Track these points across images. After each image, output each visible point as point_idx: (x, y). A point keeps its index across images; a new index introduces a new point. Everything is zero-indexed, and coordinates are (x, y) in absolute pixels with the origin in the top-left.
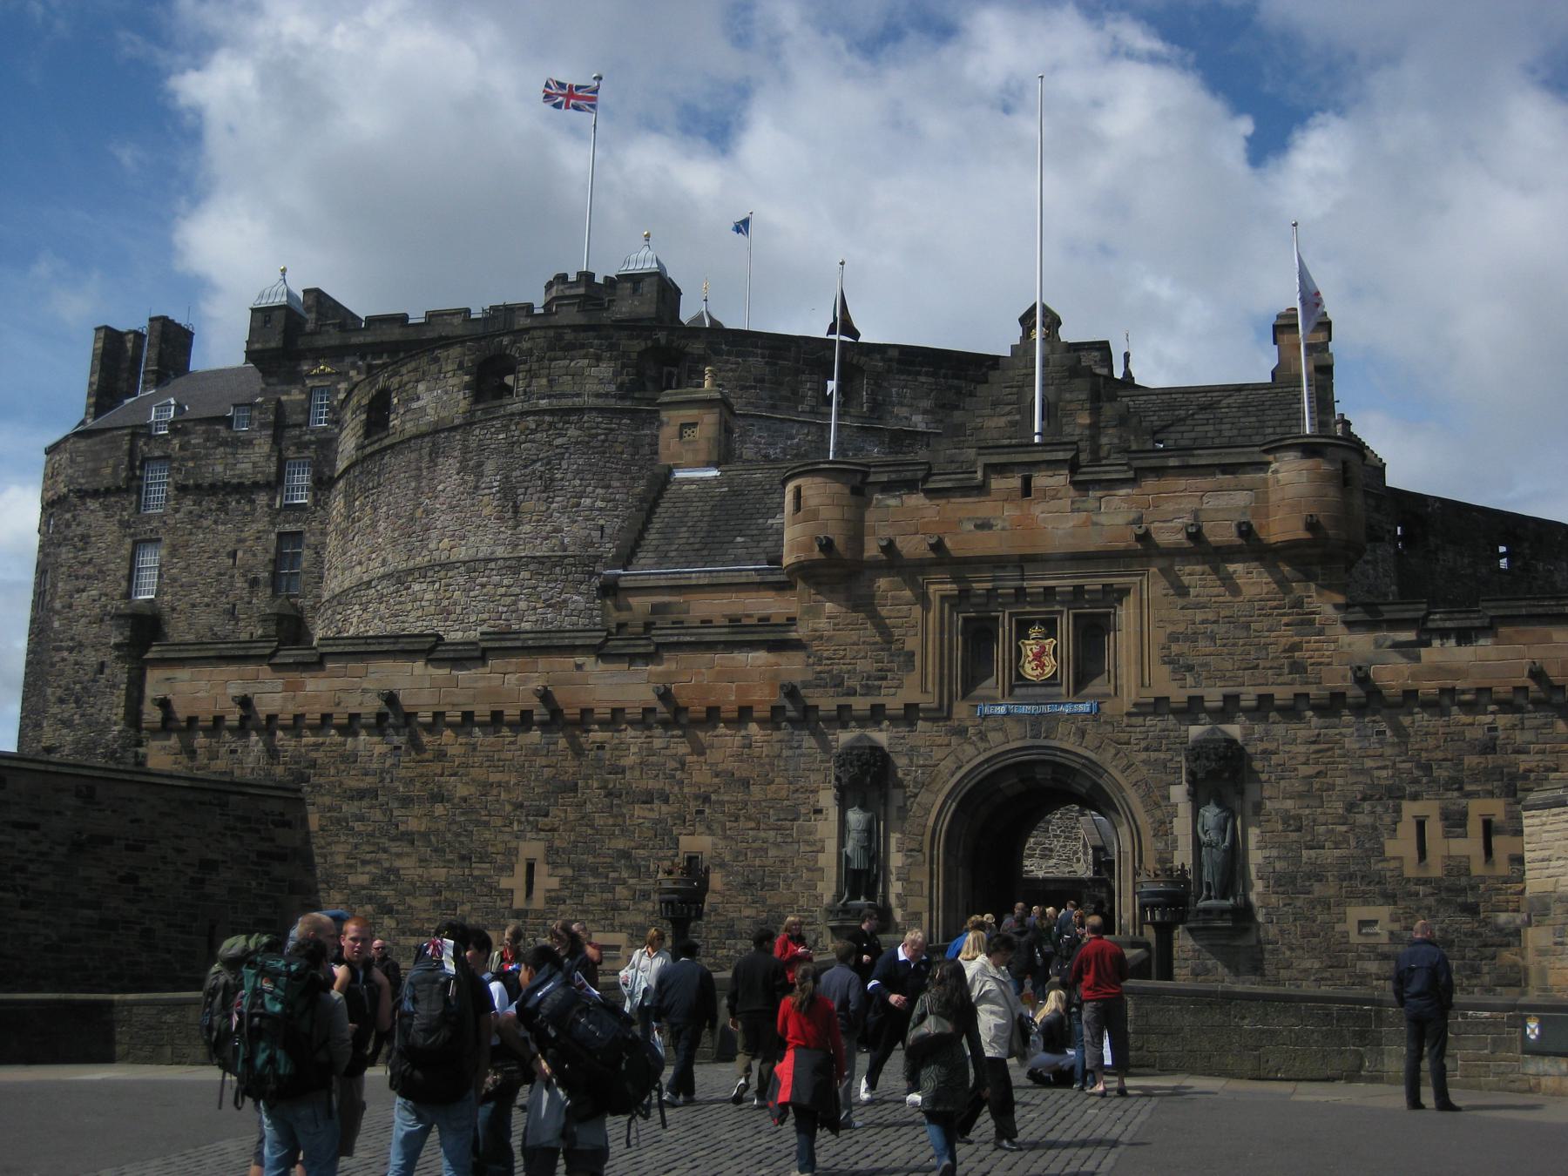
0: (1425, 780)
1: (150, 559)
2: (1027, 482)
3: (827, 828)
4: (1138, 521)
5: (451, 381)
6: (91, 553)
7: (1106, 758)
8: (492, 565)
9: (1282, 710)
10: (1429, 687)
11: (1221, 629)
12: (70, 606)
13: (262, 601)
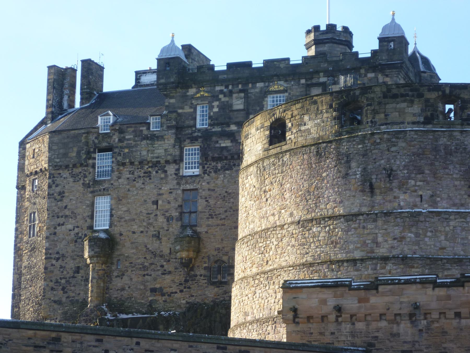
1: (103, 204)
5: (325, 115)
6: (66, 201)
8: (361, 217)
12: (55, 234)
13: (175, 227)
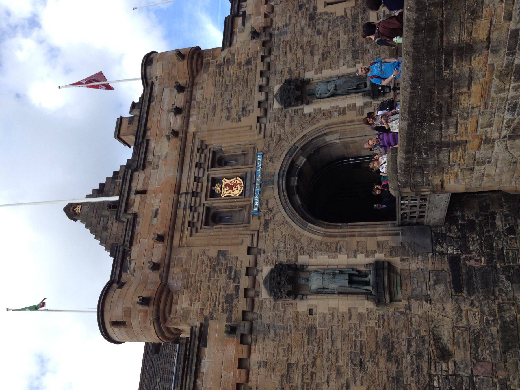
0: (307, 6)
2: (138, 192)
3: (322, 305)
4: (168, 137)
7: (287, 146)
9: (269, 68)
10: (265, 9)
11: (227, 97)
